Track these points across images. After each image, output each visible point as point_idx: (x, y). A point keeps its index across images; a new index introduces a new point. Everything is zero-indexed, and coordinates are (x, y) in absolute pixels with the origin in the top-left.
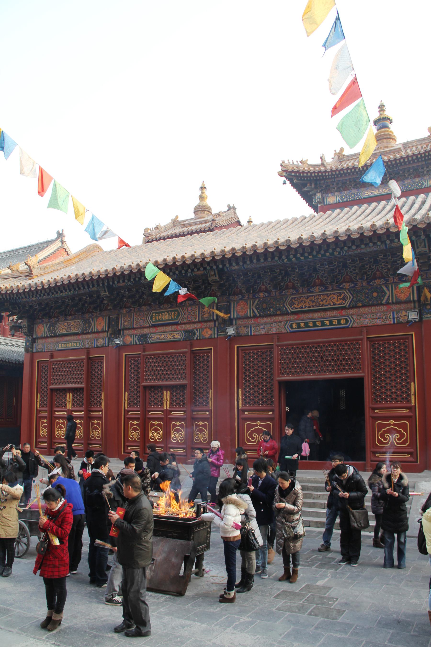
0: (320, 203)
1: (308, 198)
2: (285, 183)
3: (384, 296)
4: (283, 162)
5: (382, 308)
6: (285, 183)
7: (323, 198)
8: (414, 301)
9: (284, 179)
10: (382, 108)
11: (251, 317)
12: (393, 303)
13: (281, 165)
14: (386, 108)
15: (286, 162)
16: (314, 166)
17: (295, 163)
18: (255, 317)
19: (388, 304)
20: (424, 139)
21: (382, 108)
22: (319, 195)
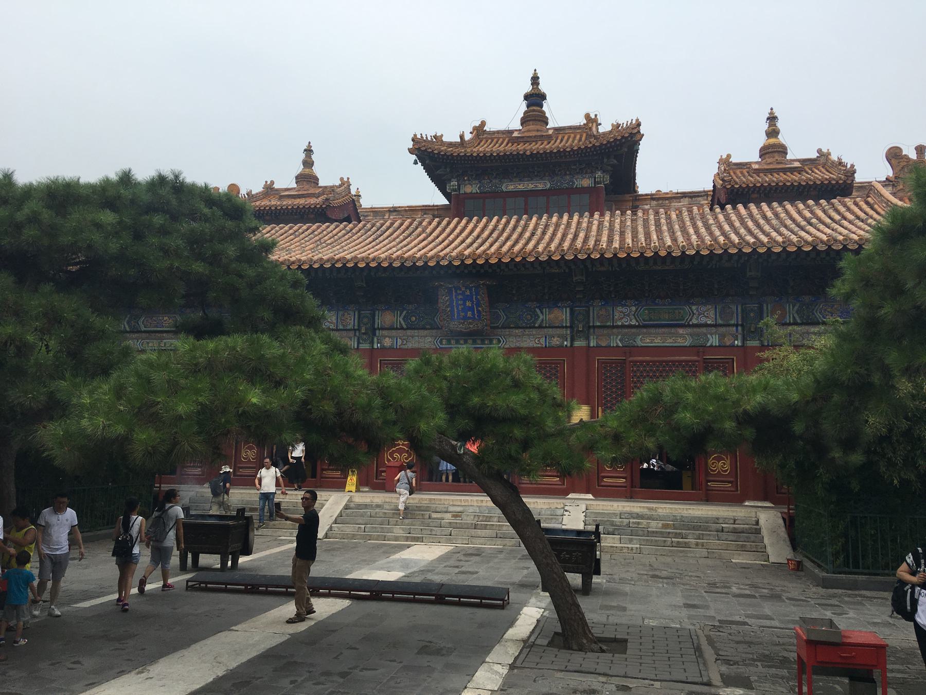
0: (455, 190)
1: (440, 183)
2: (416, 163)
3: (537, 319)
4: (415, 135)
5: (534, 331)
6: (416, 163)
7: (459, 186)
8: (566, 327)
9: (414, 157)
10: (535, 80)
11: (397, 329)
12: (546, 327)
13: (413, 140)
14: (541, 81)
15: (419, 136)
16: (451, 144)
17: (429, 139)
18: (402, 328)
19: (540, 327)
20: (579, 128)
21: (535, 80)
22: (454, 183)
